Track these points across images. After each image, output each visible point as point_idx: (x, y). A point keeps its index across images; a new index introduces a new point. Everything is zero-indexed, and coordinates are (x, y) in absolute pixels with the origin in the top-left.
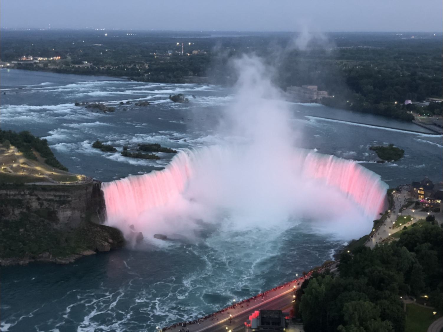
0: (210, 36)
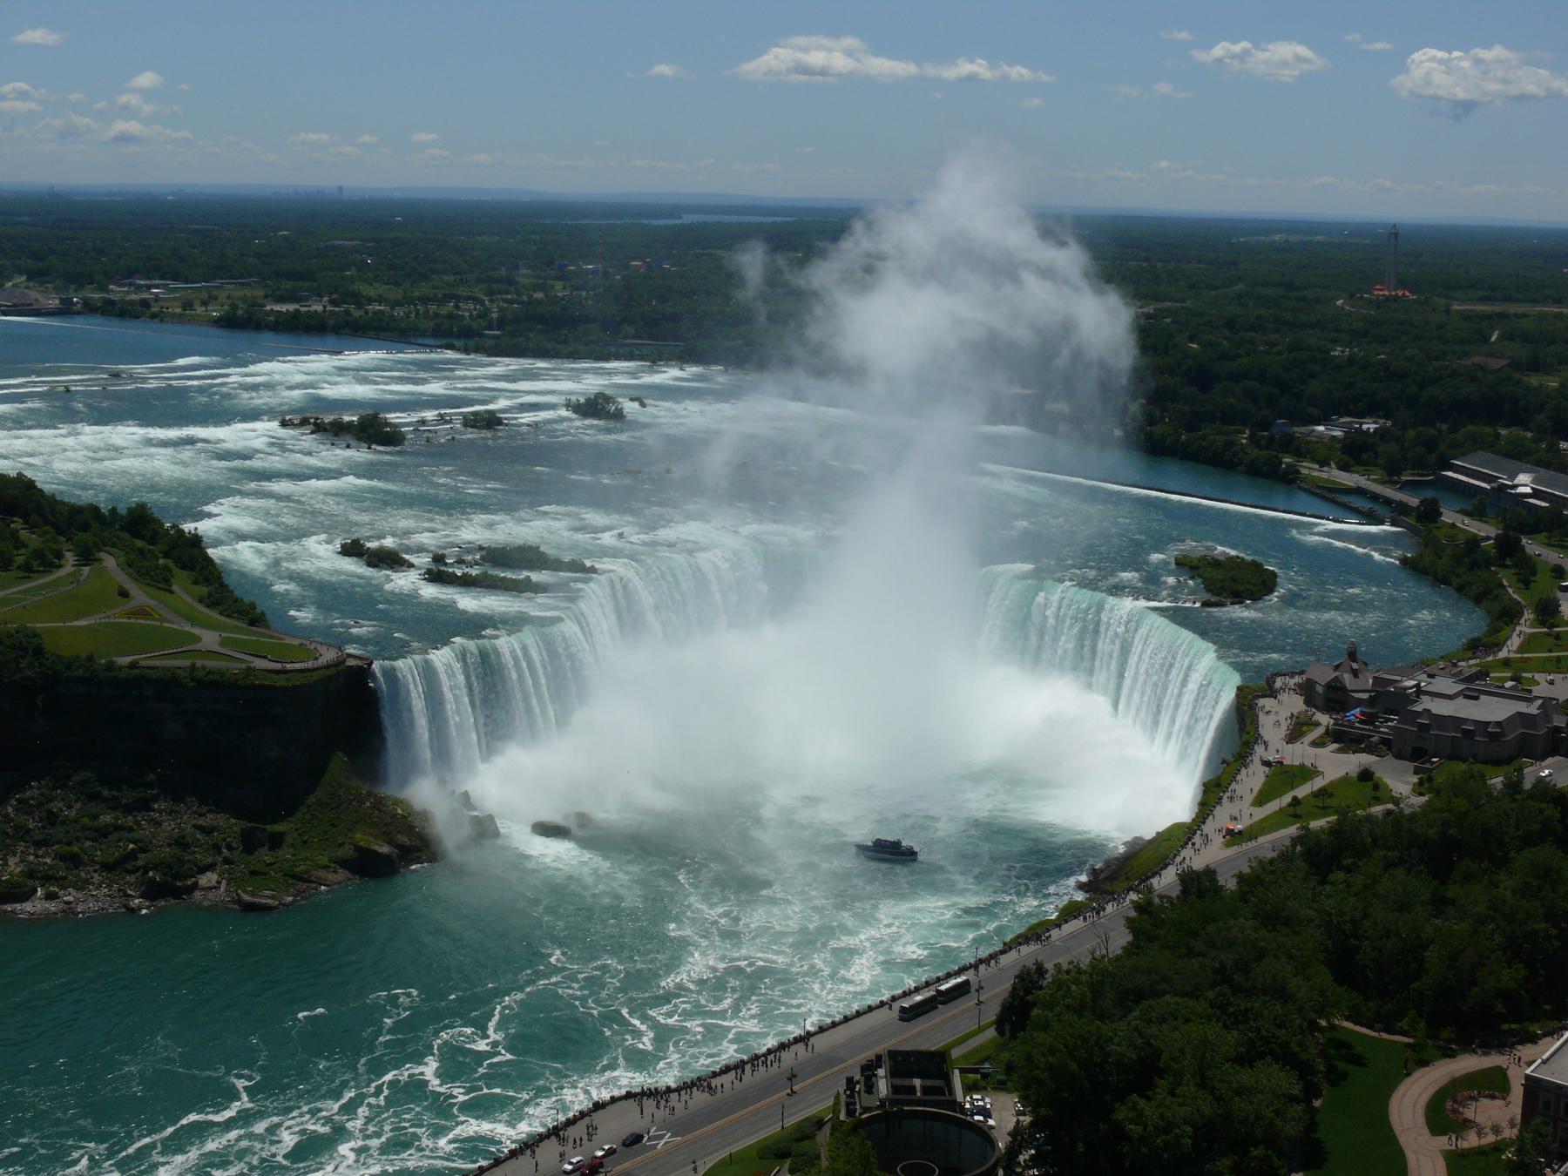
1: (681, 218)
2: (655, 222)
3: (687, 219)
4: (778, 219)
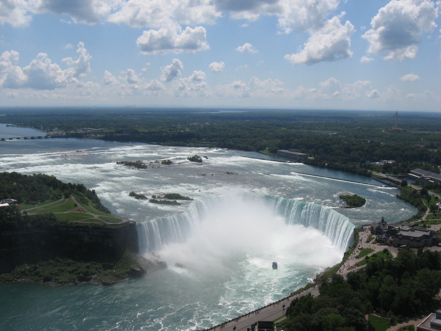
0: (219, 111)
1: (219, 111)
2: (212, 113)
3: (221, 112)
4: (243, 112)
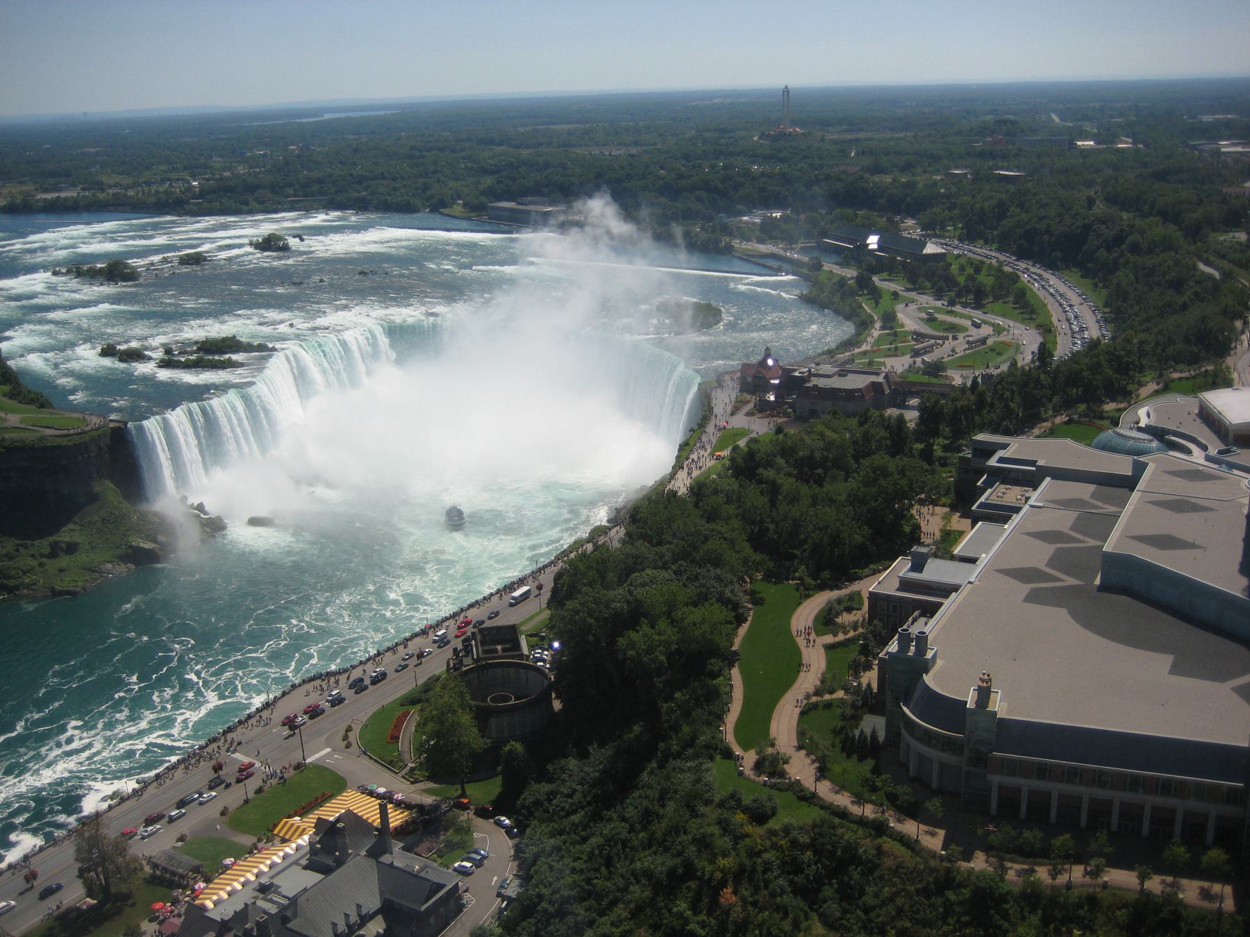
0: (322, 116)
2: (304, 120)
3: (327, 117)
4: (389, 112)
